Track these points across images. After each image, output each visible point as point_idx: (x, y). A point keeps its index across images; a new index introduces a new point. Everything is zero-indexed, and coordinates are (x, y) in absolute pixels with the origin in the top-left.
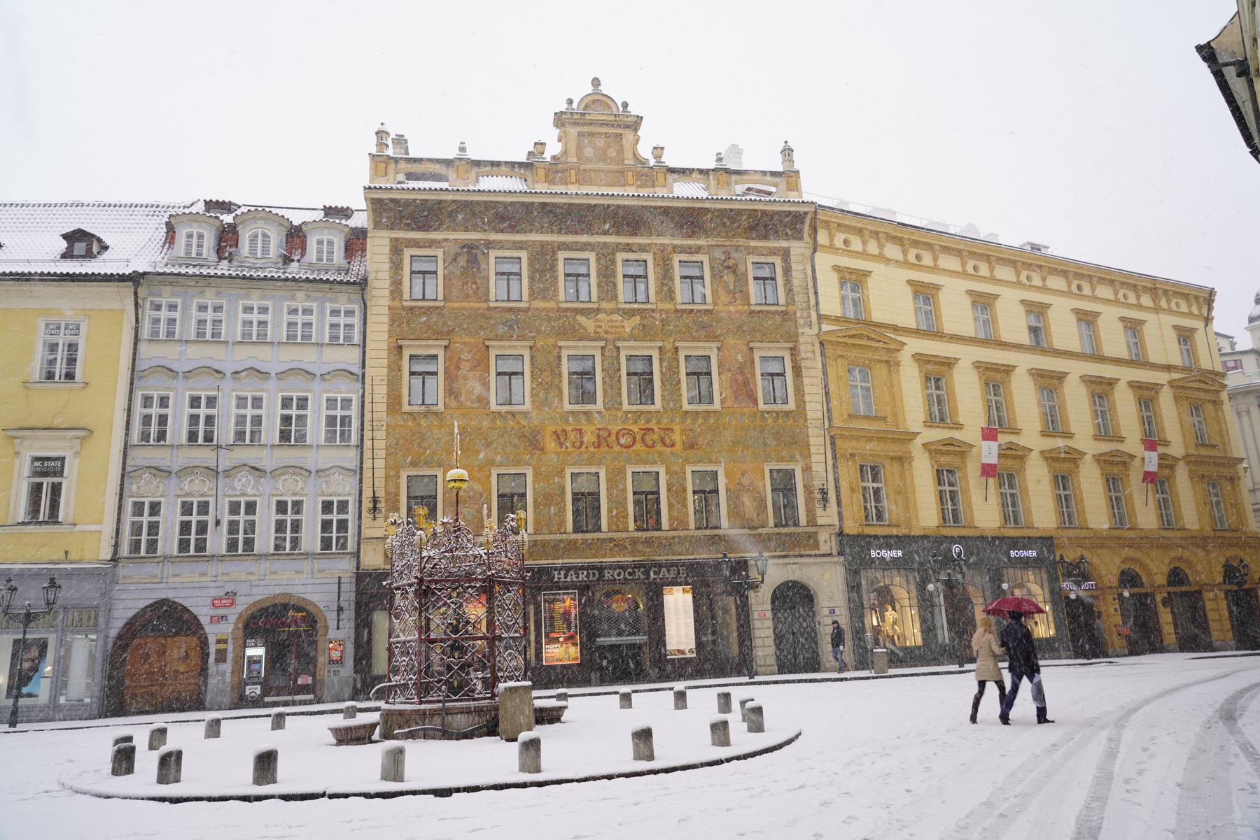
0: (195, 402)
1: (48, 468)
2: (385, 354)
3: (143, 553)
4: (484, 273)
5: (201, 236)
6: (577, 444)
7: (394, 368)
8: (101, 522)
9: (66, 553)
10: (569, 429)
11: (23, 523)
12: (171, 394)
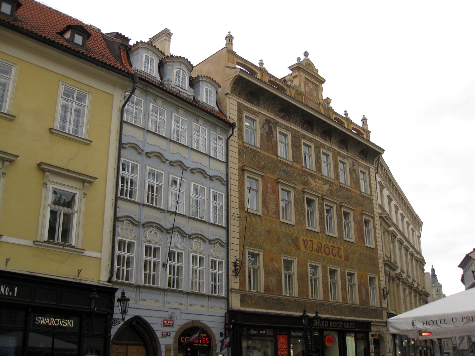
1: (64, 202)
2: (237, 172)
4: (274, 139)
6: (311, 249)
7: (241, 184)
9: (80, 271)
10: (308, 239)
11: (45, 242)
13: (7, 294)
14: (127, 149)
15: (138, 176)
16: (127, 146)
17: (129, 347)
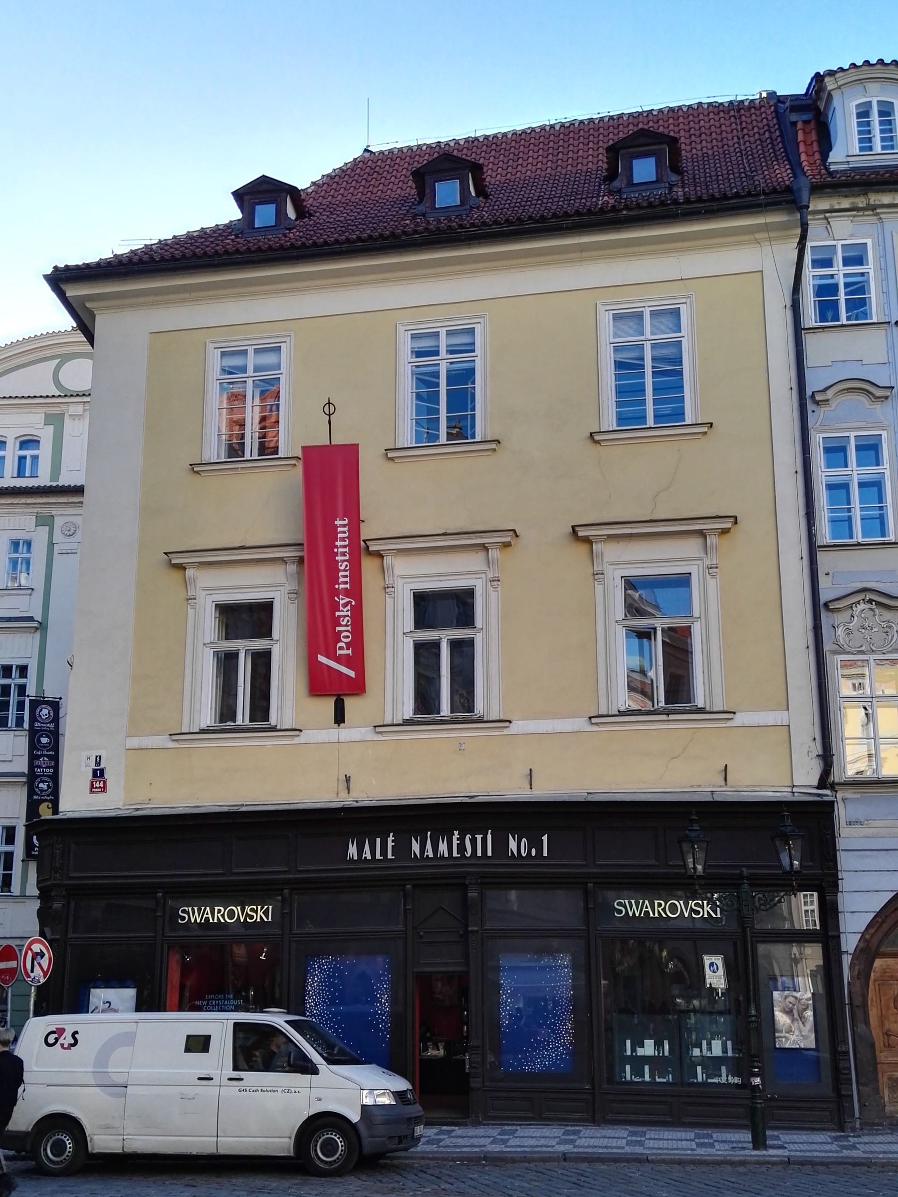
13: (524, 855)
14: (834, 404)
15: (886, 465)
16: (830, 394)
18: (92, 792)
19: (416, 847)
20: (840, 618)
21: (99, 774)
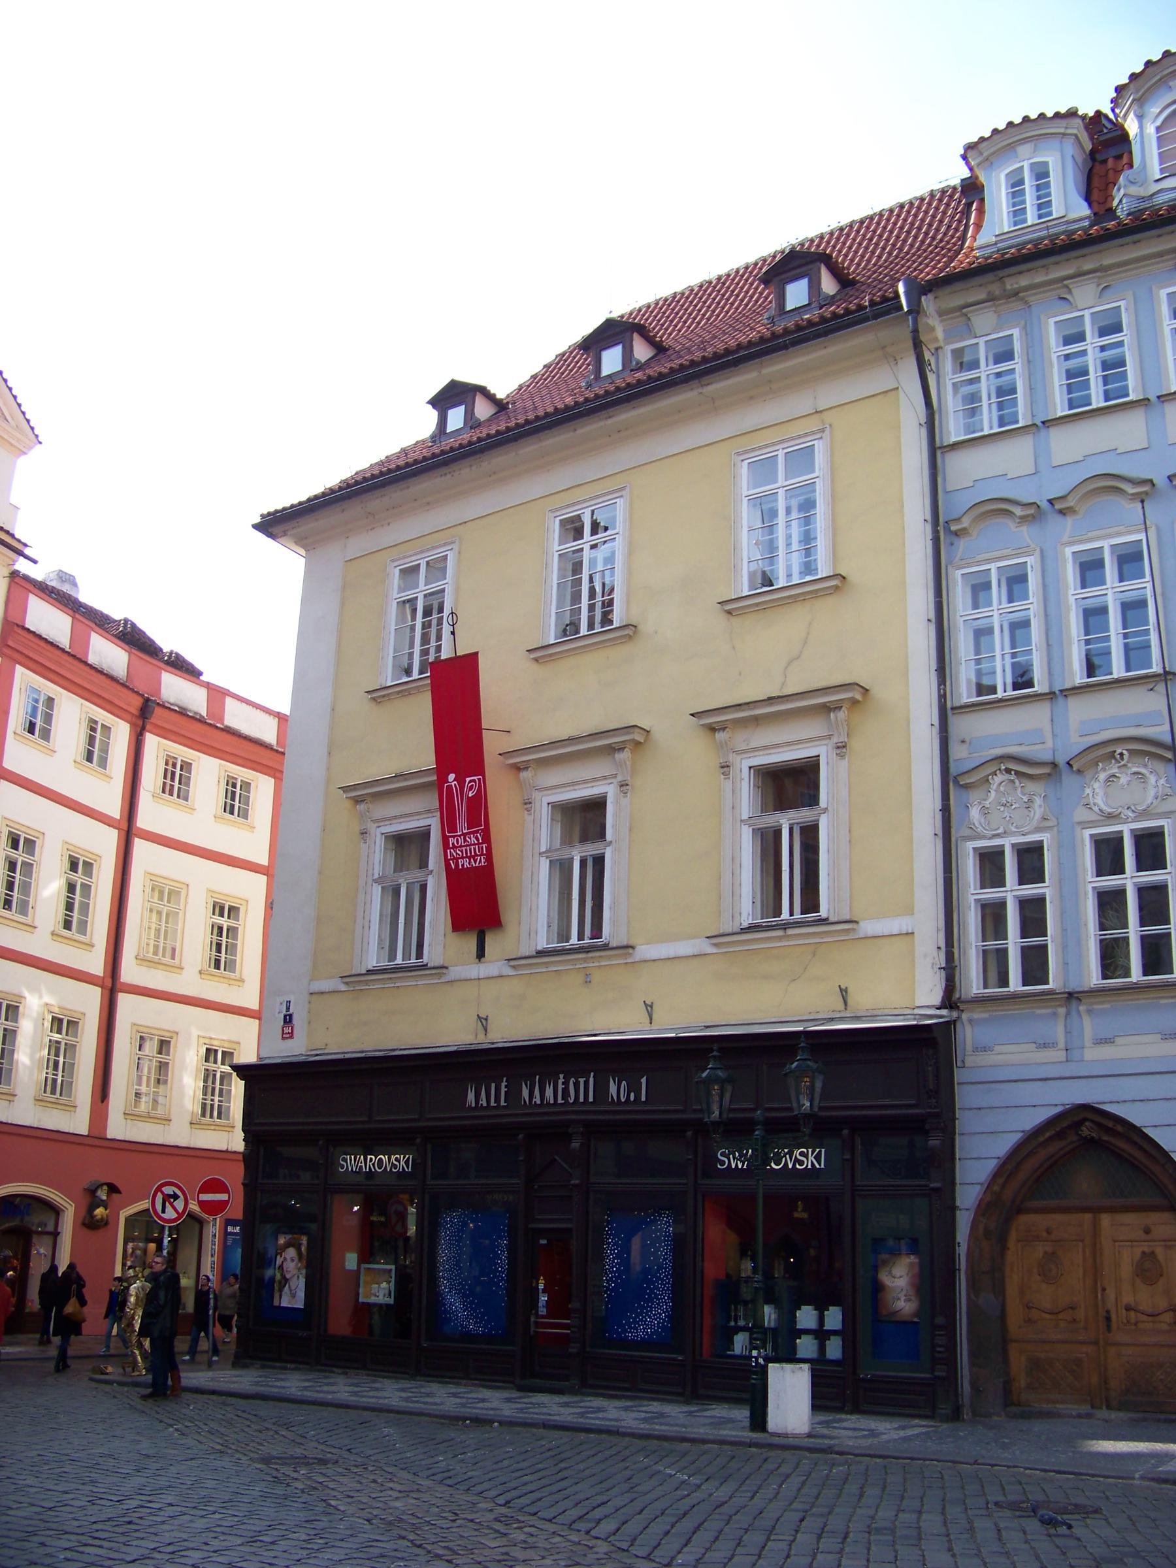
0: (1090, 569)
3: (1015, 983)
5: (1041, 173)
8: (909, 911)
9: (844, 992)
11: (752, 928)
12: (1031, 561)
13: (623, 1100)
17: (1105, 1219)
18: (283, 1038)
19: (525, 1093)
20: (974, 796)
21: (288, 1020)
